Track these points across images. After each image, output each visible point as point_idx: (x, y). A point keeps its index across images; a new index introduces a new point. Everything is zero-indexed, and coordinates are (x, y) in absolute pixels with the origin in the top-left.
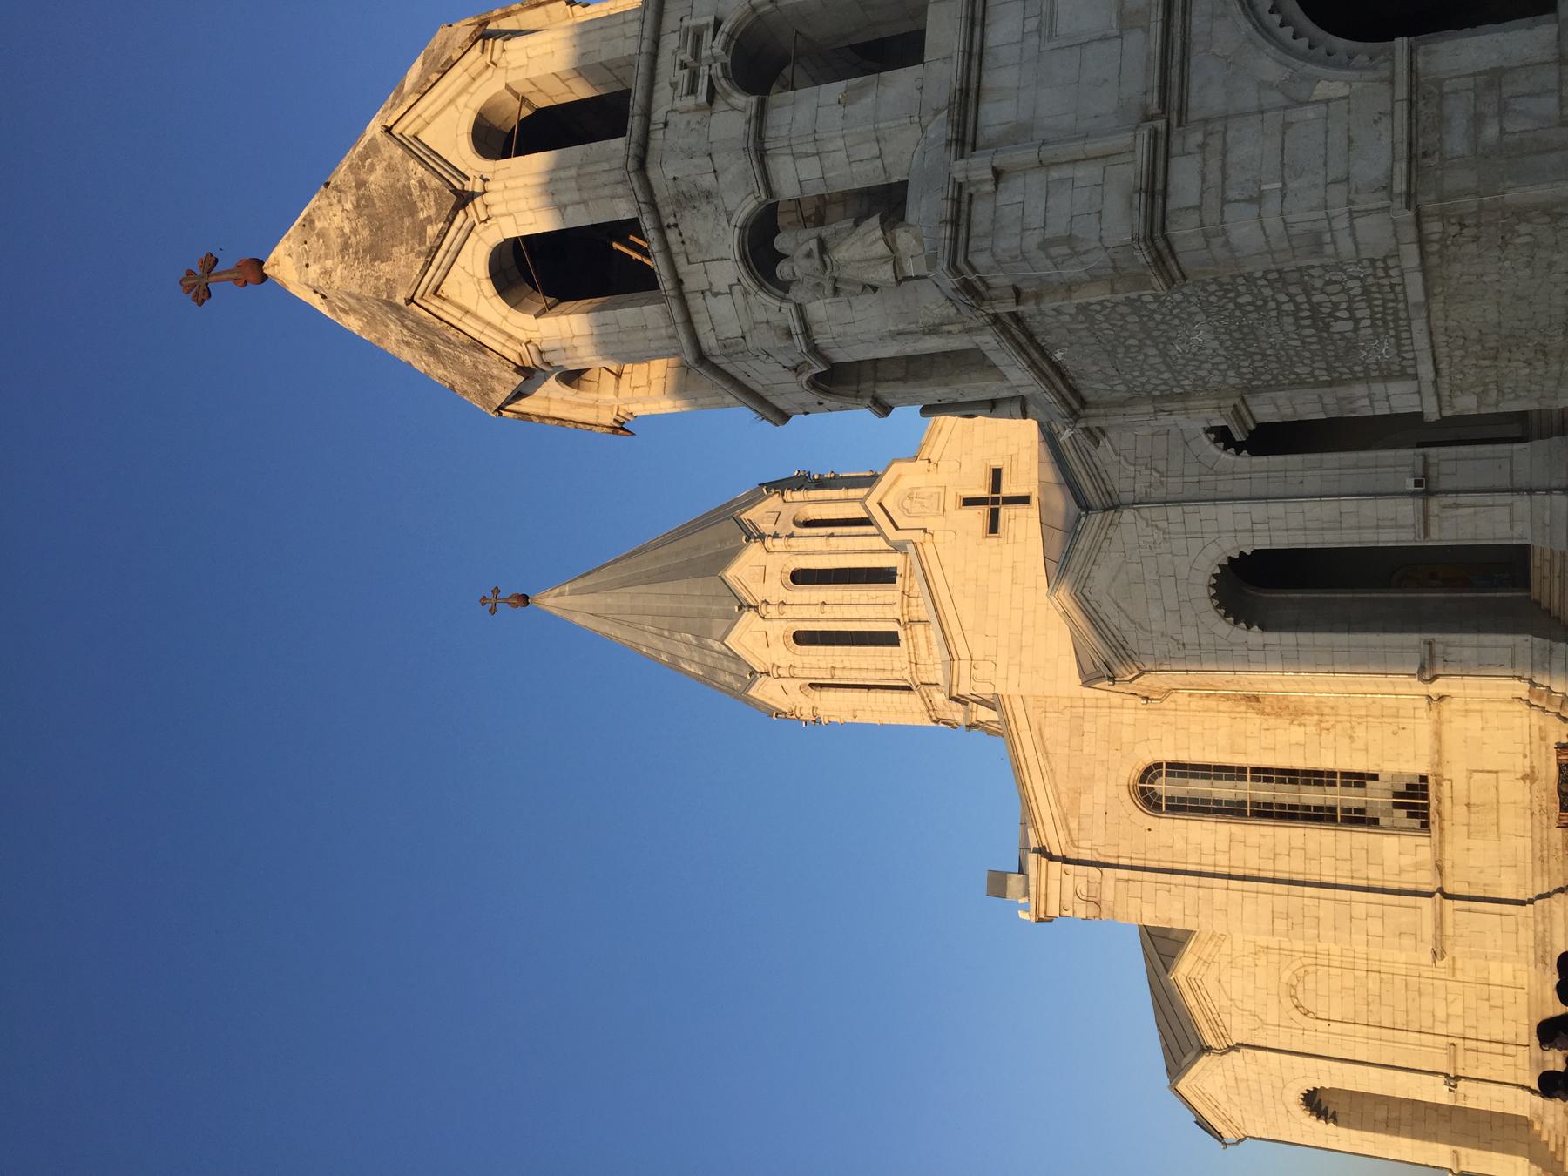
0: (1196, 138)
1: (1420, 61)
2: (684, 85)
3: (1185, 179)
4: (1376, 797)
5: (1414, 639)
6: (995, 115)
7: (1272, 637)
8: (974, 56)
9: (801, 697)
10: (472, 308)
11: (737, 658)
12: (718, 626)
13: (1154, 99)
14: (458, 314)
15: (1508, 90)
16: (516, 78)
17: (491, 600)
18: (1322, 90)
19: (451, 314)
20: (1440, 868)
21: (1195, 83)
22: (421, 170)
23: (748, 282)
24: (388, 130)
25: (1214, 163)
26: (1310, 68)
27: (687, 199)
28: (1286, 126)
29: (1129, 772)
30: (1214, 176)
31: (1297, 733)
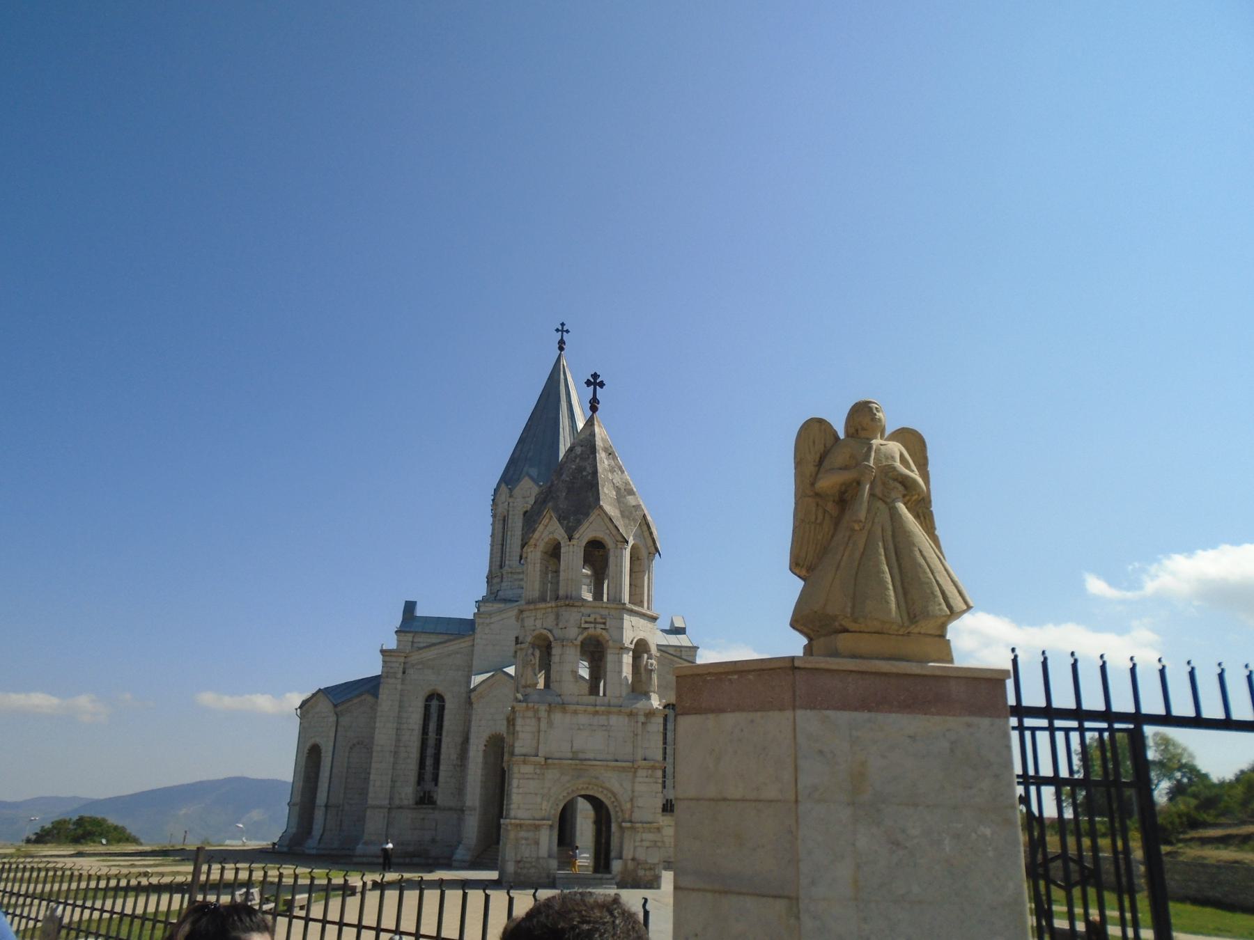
0: (538, 771)
2: (588, 619)
4: (429, 786)
5: (477, 804)
6: (557, 717)
7: (481, 754)
9: (500, 510)
11: (519, 480)
12: (534, 472)
16: (611, 554)
17: (562, 329)
18: (545, 803)
19: (545, 521)
20: (400, 807)
27: (557, 617)
29: (440, 690)
31: (454, 757)
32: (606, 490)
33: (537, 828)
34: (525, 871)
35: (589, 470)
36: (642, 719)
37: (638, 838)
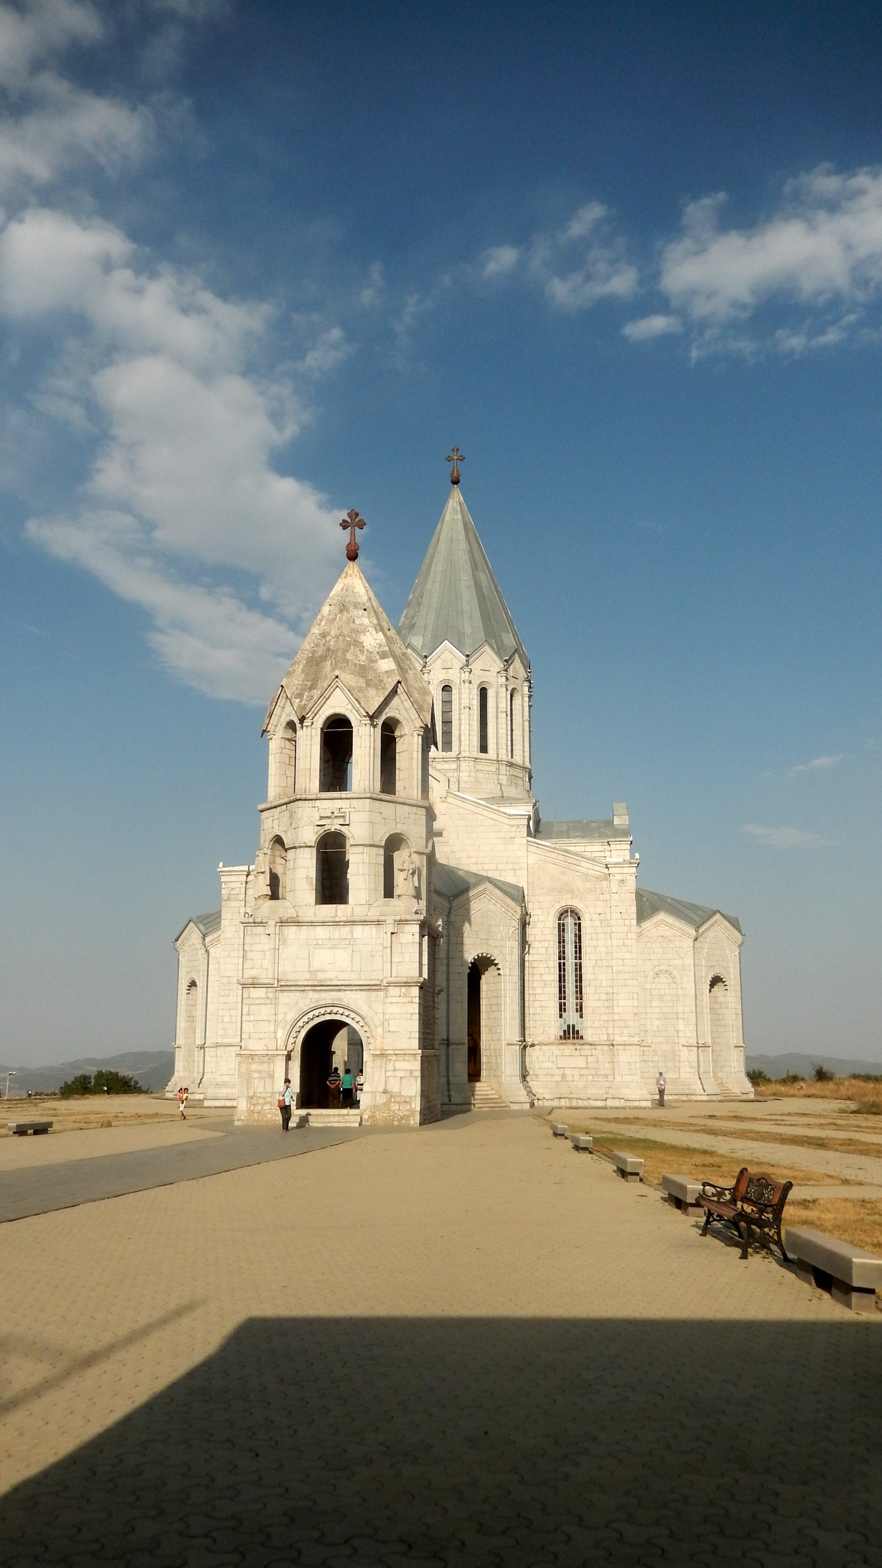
0: (271, 995)
1: (280, 1057)
3: (259, 993)
6: (291, 932)
8: (312, 924)
10: (285, 710)
13: (283, 983)
14: (282, 705)
15: (267, 1080)
21: (291, 994)
22: (315, 697)
23: (273, 835)
24: (337, 677)
25: (262, 1001)
26: (288, 1027)
28: (269, 1021)
30: (258, 1001)
32: (349, 656)
33: (271, 1058)
34: (259, 1108)
35: (333, 634)
36: (391, 929)
37: (390, 1066)
